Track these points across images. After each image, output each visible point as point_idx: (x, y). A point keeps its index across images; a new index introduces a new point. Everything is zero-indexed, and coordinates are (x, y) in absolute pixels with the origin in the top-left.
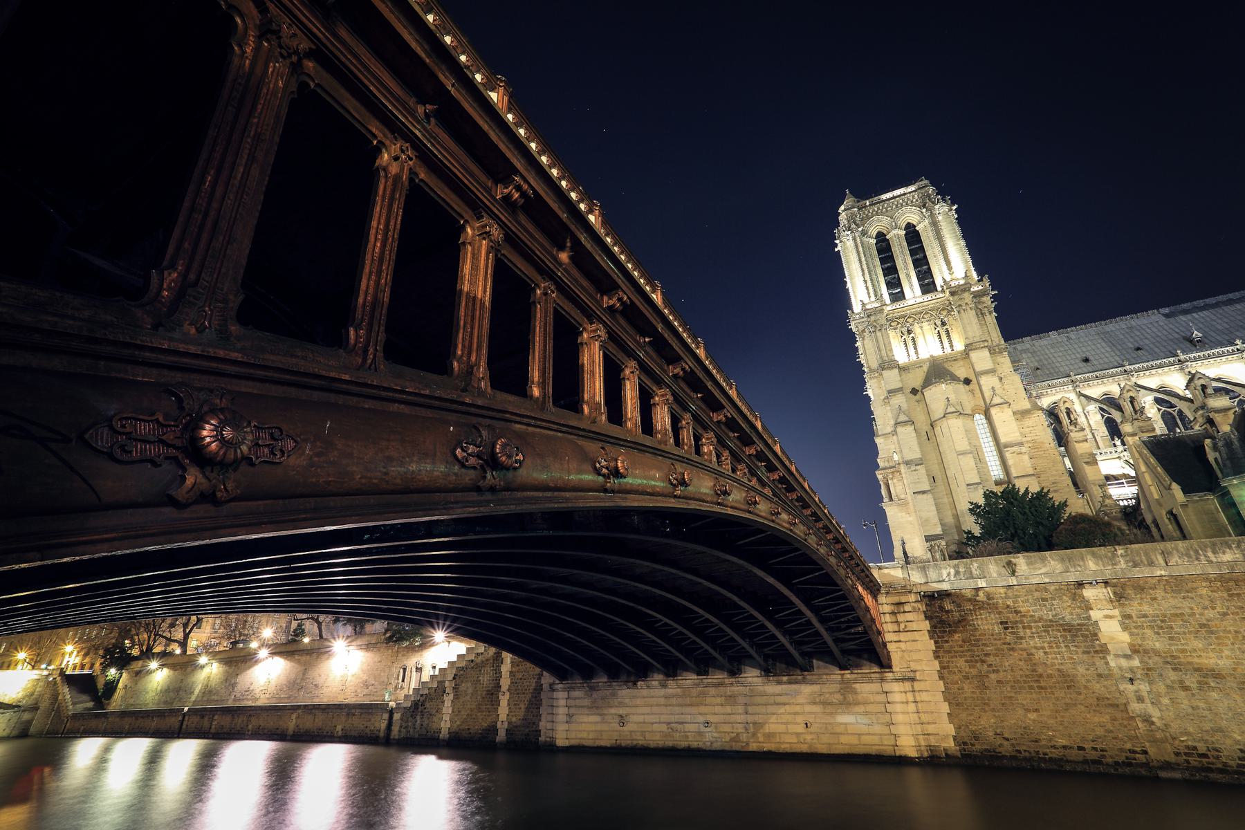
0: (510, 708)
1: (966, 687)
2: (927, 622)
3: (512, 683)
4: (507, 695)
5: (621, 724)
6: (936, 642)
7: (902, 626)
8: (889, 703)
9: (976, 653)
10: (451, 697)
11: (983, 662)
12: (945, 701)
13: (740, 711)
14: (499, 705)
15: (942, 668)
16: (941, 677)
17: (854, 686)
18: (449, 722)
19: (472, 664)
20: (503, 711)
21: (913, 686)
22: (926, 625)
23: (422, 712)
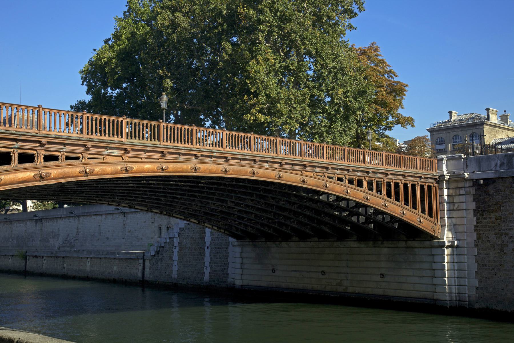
0: (211, 258)
1: (491, 253)
2: (474, 203)
3: (212, 240)
6: (477, 219)
7: (456, 206)
8: (435, 262)
9: (503, 228)
11: (506, 234)
12: (476, 262)
14: (205, 255)
15: (478, 238)
16: (476, 246)
18: (177, 266)
22: (473, 206)
23: (161, 259)
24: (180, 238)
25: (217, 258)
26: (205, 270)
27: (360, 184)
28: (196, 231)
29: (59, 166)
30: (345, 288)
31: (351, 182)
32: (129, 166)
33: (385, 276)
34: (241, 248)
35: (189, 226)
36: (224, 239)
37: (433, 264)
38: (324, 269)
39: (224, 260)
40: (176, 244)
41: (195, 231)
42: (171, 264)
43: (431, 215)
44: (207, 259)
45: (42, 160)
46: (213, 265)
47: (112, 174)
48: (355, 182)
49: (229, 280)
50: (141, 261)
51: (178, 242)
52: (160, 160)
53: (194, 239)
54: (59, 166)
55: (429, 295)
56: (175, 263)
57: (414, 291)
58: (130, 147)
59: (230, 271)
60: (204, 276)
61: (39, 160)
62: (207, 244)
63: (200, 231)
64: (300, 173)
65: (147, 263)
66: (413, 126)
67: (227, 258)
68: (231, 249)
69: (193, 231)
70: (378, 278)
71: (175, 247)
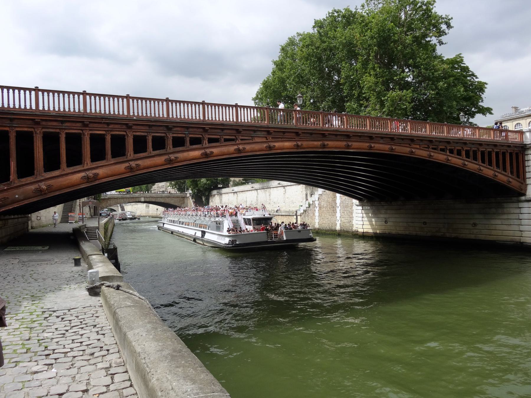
0: (341, 214)
4: (339, 207)
5: (386, 222)
14: (336, 212)
17: (503, 204)
18: (318, 220)
20: (338, 215)
23: (308, 215)
26: (337, 222)
27: (459, 153)
29: (219, 146)
30: (442, 234)
31: (451, 151)
32: (272, 144)
35: (325, 193)
37: (520, 215)
40: (317, 205)
43: (518, 176)
45: (207, 143)
46: (343, 219)
47: (259, 151)
48: (455, 152)
49: (354, 229)
50: (295, 217)
52: (296, 139)
54: (219, 146)
55: (517, 239)
56: (317, 218)
58: (272, 130)
59: (354, 222)
61: (205, 142)
62: (338, 205)
63: (333, 196)
64: (408, 146)
65: (299, 217)
66: (491, 113)
67: (352, 214)
68: (355, 207)
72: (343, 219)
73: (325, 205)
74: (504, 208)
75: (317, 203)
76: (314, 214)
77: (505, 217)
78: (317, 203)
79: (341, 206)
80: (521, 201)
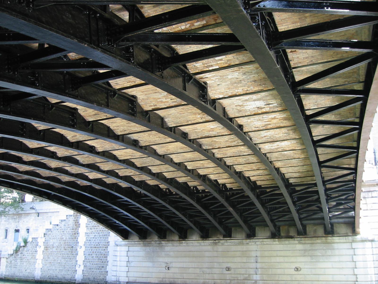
0: (85, 257)
10: (42, 248)
13: (252, 261)
14: (77, 254)
19: (57, 227)
21: (372, 245)
23: (21, 257)
24: (45, 239)
25: (93, 257)
26: (77, 268)
28: (66, 232)
33: (299, 269)
34: (128, 247)
36: (102, 239)
37: (354, 256)
38: (229, 265)
39: (101, 258)
41: (65, 232)
42: (34, 262)
44: (80, 258)
46: (88, 263)
51: (44, 242)
53: (64, 239)
57: (333, 281)
60: (76, 273)
63: (72, 232)
69: (63, 231)
70: (293, 272)
71: (39, 247)
72: (88, 264)
73: (57, 244)
74: (334, 249)
75: (41, 241)
76: (34, 257)
77: (336, 259)
78: (41, 241)
79: (87, 246)
80: (356, 241)
